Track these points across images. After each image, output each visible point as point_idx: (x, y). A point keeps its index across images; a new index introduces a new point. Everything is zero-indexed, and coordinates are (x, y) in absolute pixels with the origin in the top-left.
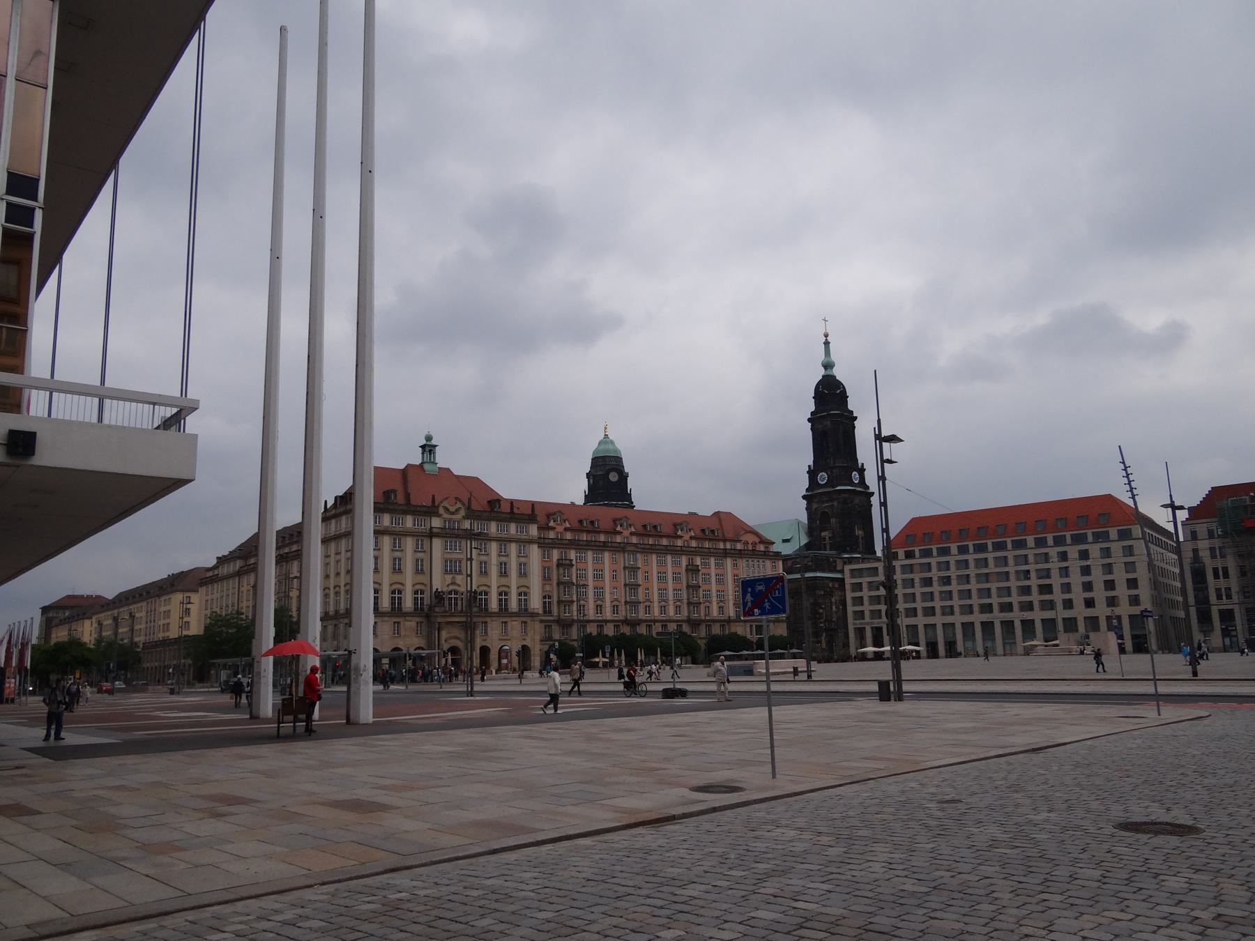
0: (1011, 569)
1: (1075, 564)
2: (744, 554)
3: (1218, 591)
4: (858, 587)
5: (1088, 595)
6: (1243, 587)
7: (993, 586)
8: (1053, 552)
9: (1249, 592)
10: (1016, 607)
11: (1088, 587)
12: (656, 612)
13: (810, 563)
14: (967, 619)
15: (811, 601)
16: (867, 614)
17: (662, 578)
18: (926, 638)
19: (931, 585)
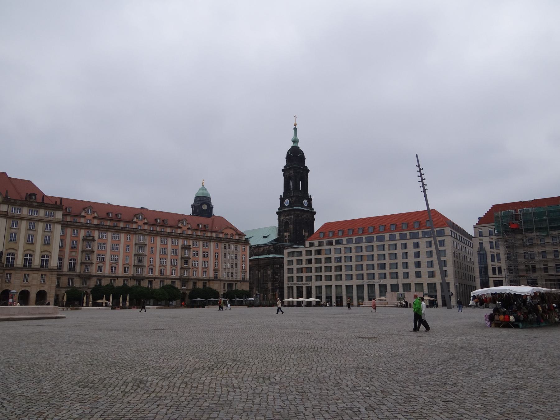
0: (375, 253)
1: (411, 250)
2: (223, 241)
3: (494, 269)
4: (291, 262)
5: (418, 270)
6: (509, 267)
7: (365, 263)
8: (399, 243)
9: (512, 270)
10: (376, 276)
11: (418, 265)
12: (157, 273)
13: (272, 249)
14: (349, 283)
15: (272, 271)
16: (295, 279)
17: (163, 253)
18: (326, 293)
19: (385, 269)
